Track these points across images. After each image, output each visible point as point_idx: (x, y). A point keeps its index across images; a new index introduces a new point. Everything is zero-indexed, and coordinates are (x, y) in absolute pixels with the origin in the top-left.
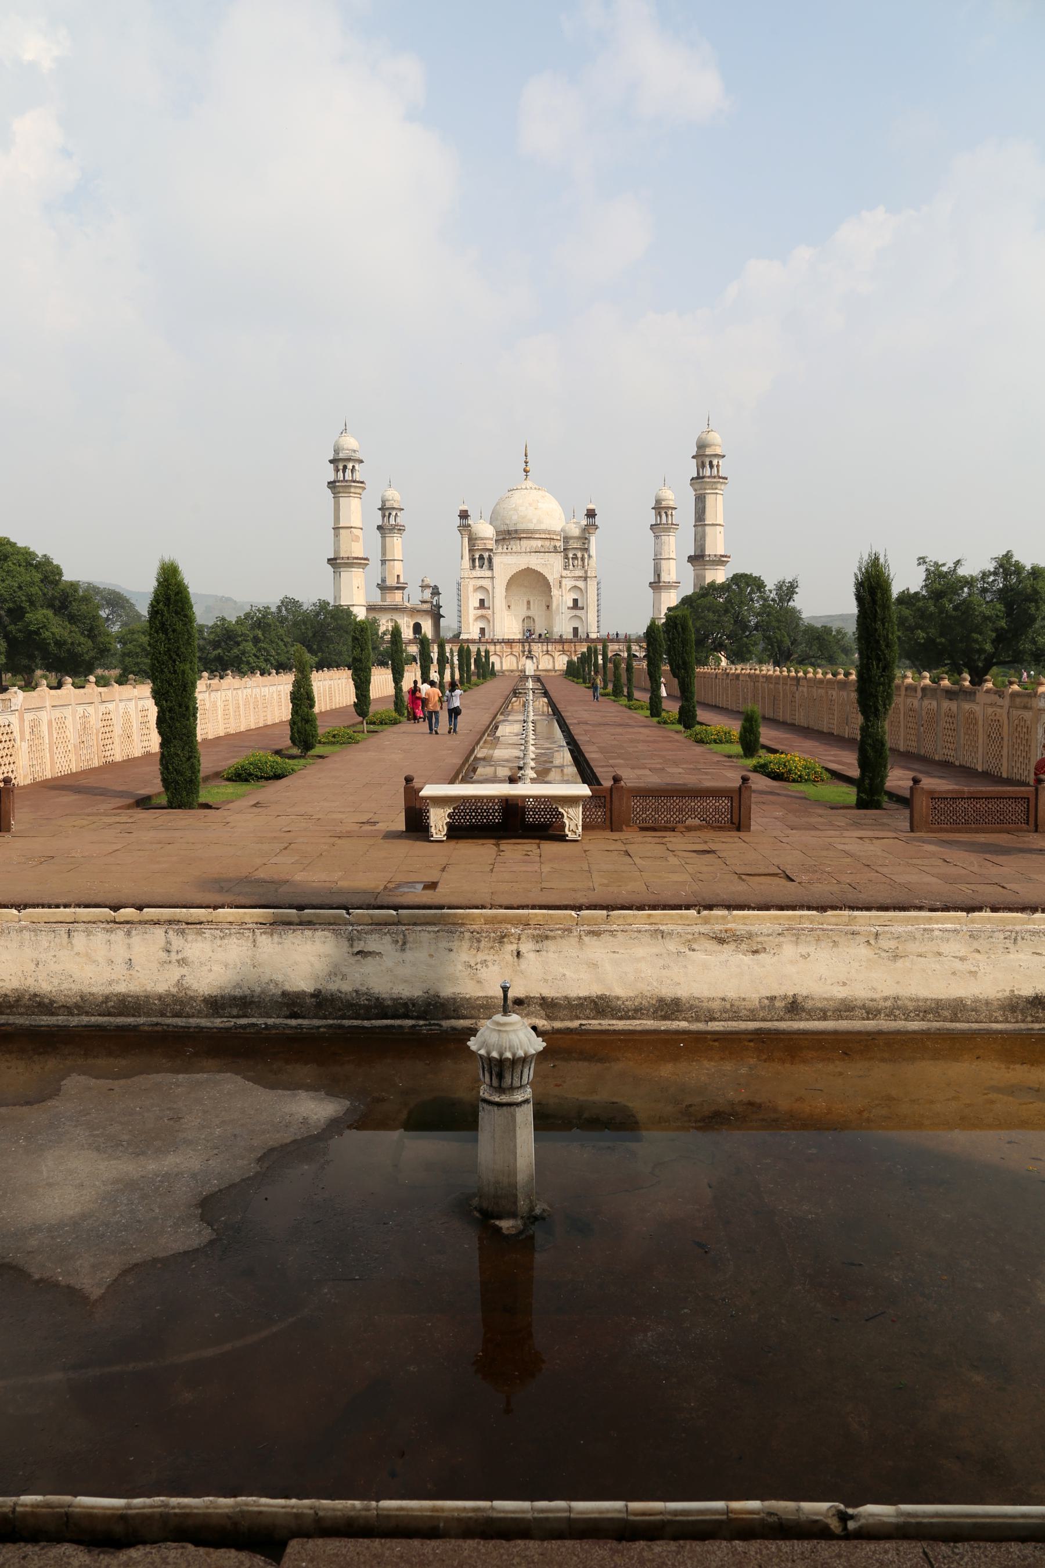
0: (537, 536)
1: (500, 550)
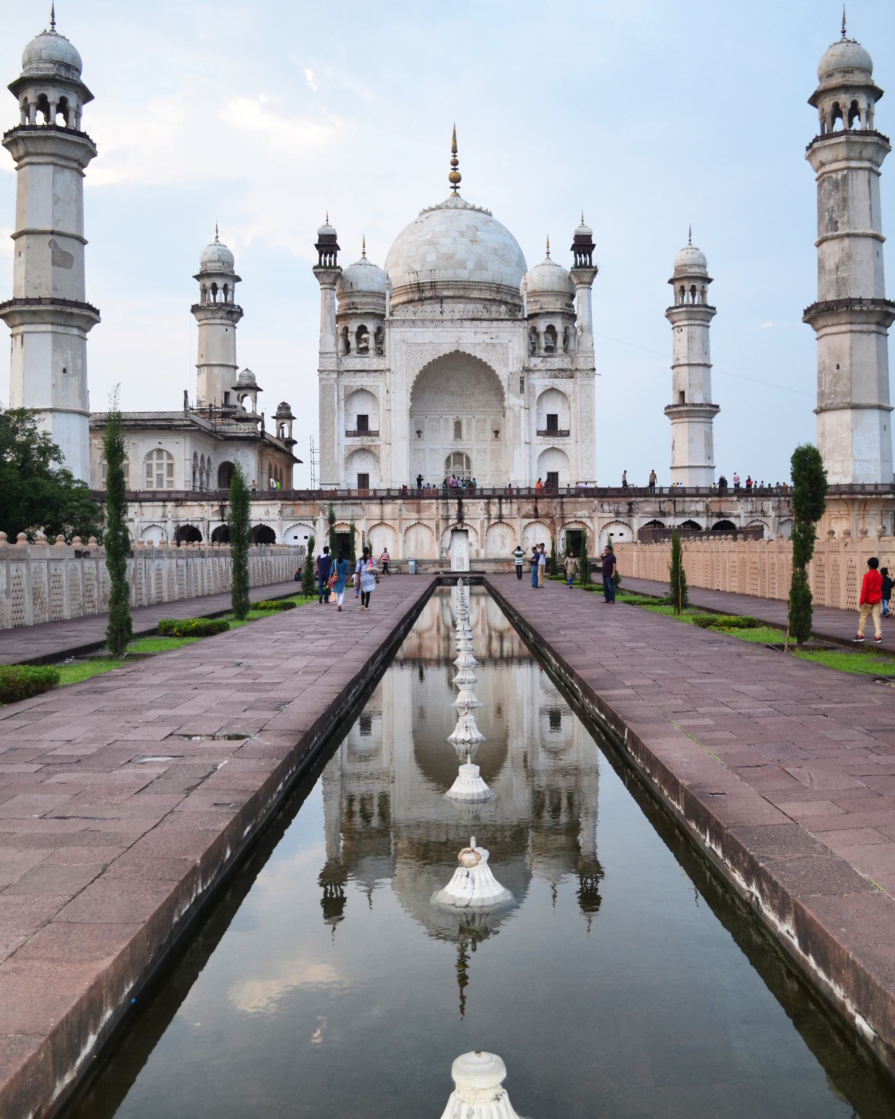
0: (475, 294)
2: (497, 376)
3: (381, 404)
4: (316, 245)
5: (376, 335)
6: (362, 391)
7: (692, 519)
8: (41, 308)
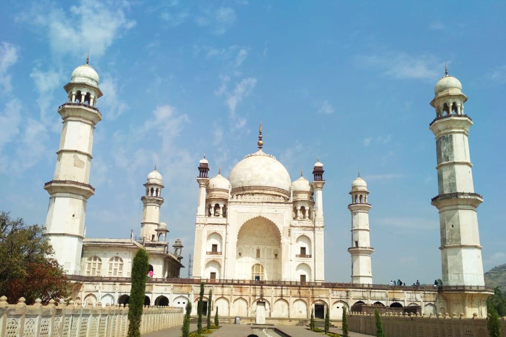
1: (235, 199)
2: (278, 229)
4: (199, 168)
5: (223, 208)
6: (215, 233)
7: (379, 301)
8: (66, 185)
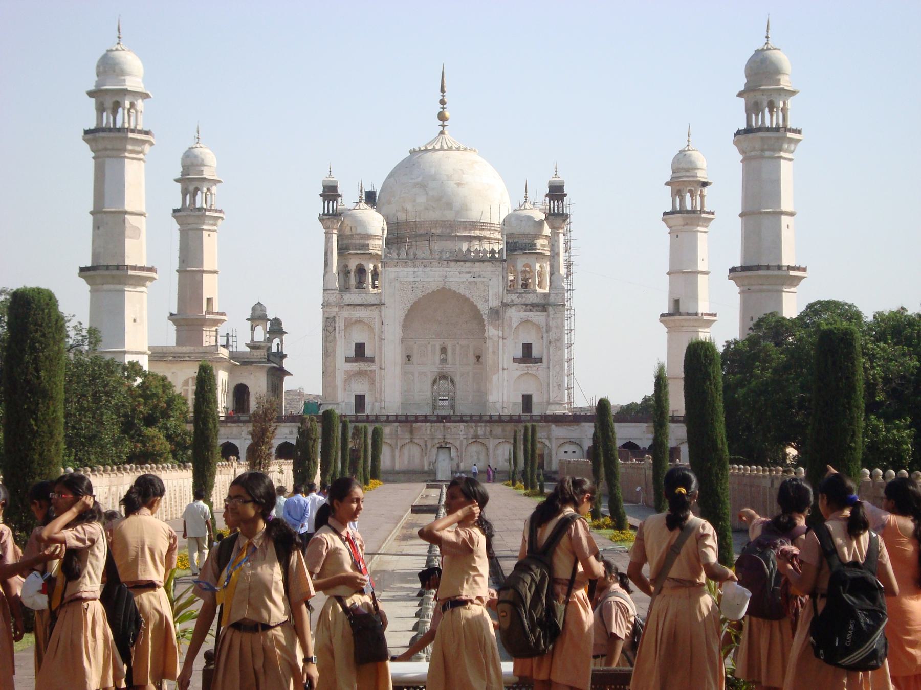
2: (479, 311)
3: (376, 330)
6: (359, 321)
